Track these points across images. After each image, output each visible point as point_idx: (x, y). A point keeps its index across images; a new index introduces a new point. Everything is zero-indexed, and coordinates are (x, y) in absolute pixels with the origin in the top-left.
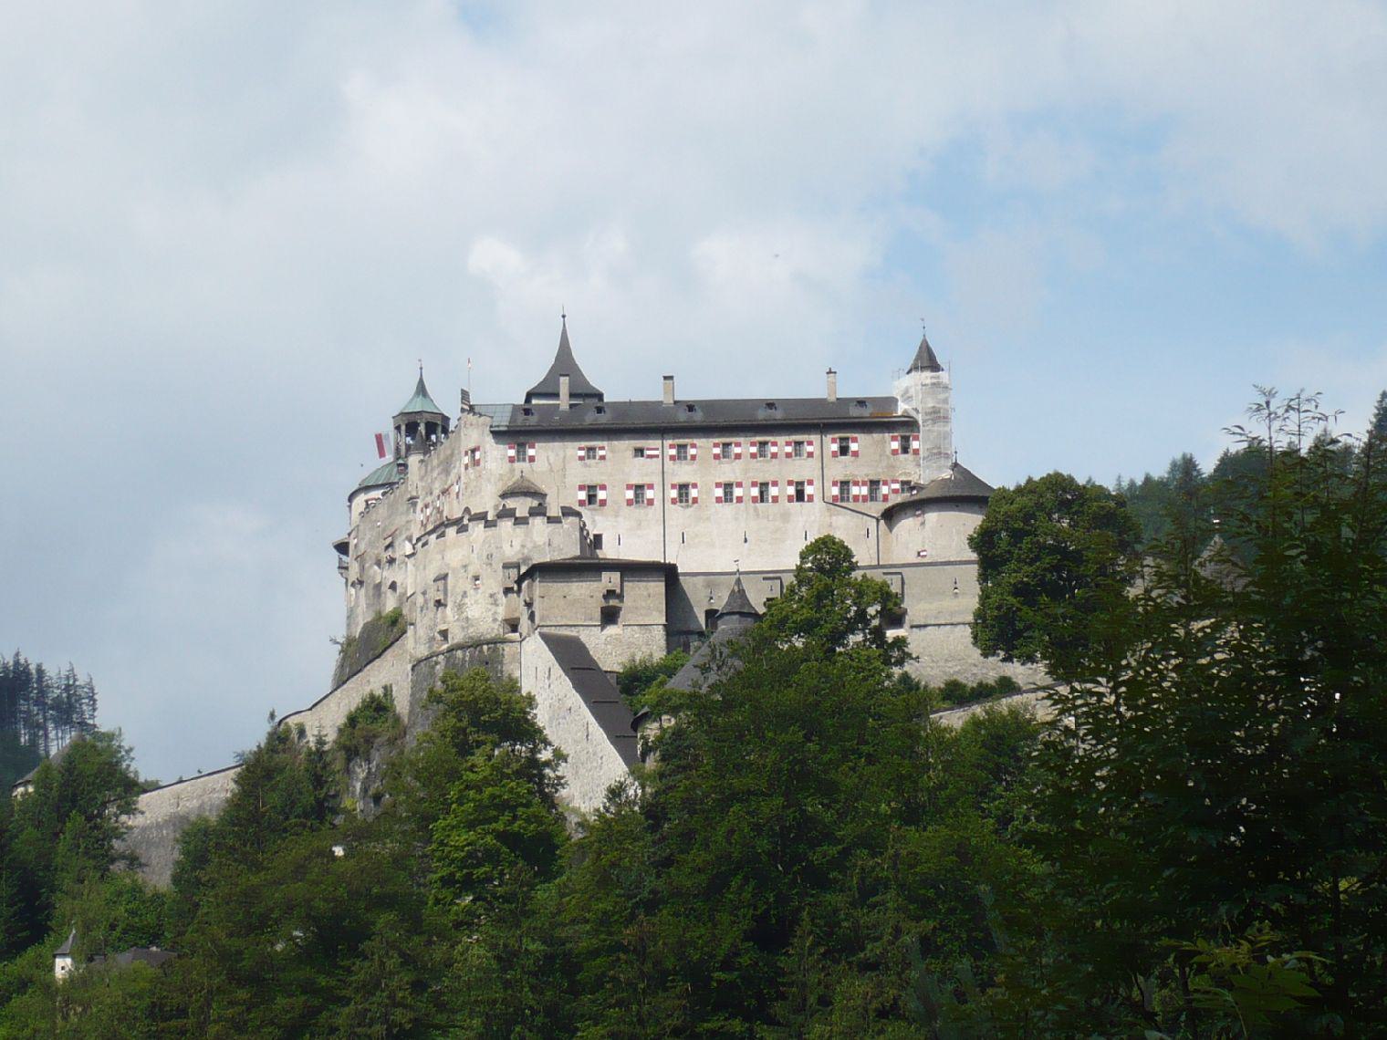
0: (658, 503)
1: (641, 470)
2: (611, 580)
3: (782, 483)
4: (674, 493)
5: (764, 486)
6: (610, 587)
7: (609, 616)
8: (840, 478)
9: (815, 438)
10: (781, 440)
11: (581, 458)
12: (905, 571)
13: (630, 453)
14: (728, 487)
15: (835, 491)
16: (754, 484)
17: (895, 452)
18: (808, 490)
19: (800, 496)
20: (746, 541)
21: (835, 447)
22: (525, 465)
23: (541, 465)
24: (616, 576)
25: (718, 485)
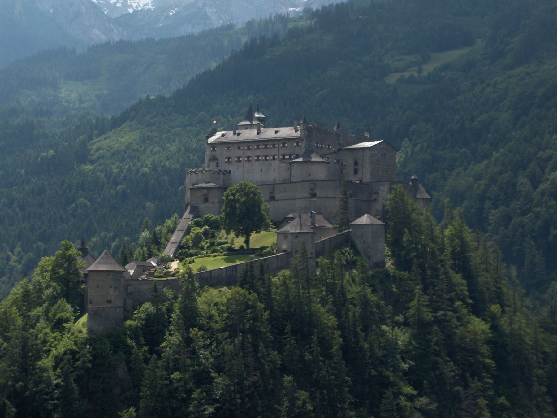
0: (243, 161)
1: (239, 153)
4: (246, 159)
5: (266, 156)
7: (206, 200)
9: (277, 142)
11: (226, 150)
14: (258, 157)
15: (281, 157)
16: (263, 156)
17: (295, 146)
18: (276, 157)
19: (274, 159)
20: (262, 171)
21: (281, 145)
22: (213, 152)
23: (218, 152)
25: (256, 156)
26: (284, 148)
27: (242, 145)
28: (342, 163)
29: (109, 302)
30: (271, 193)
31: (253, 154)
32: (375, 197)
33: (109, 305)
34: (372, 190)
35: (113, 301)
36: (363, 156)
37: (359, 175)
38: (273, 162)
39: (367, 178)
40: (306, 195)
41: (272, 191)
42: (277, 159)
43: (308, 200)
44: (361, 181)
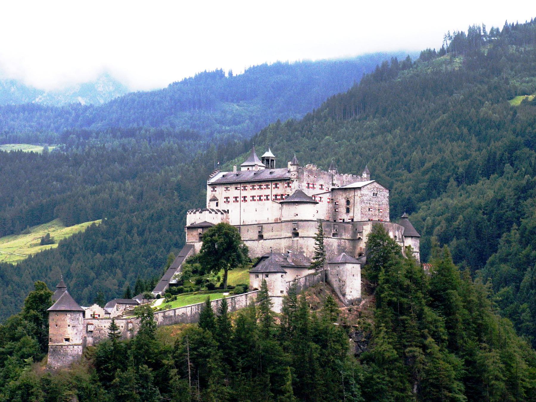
1: (236, 193)
2: (200, 231)
3: (263, 196)
6: (200, 232)
8: (275, 194)
9: (270, 184)
10: (263, 184)
12: (264, 226)
13: (234, 189)
14: (253, 197)
17: (286, 187)
19: (268, 199)
22: (214, 193)
24: (201, 230)
26: (276, 189)
27: (239, 186)
28: (335, 203)
29: (67, 340)
30: (259, 232)
31: (249, 192)
32: (359, 236)
33: (67, 343)
34: (356, 229)
35: (70, 339)
36: (354, 196)
37: (351, 214)
38: (266, 201)
39: (357, 218)
40: (290, 235)
41: (260, 230)
42: (270, 199)
43: (291, 239)
44: (352, 220)
